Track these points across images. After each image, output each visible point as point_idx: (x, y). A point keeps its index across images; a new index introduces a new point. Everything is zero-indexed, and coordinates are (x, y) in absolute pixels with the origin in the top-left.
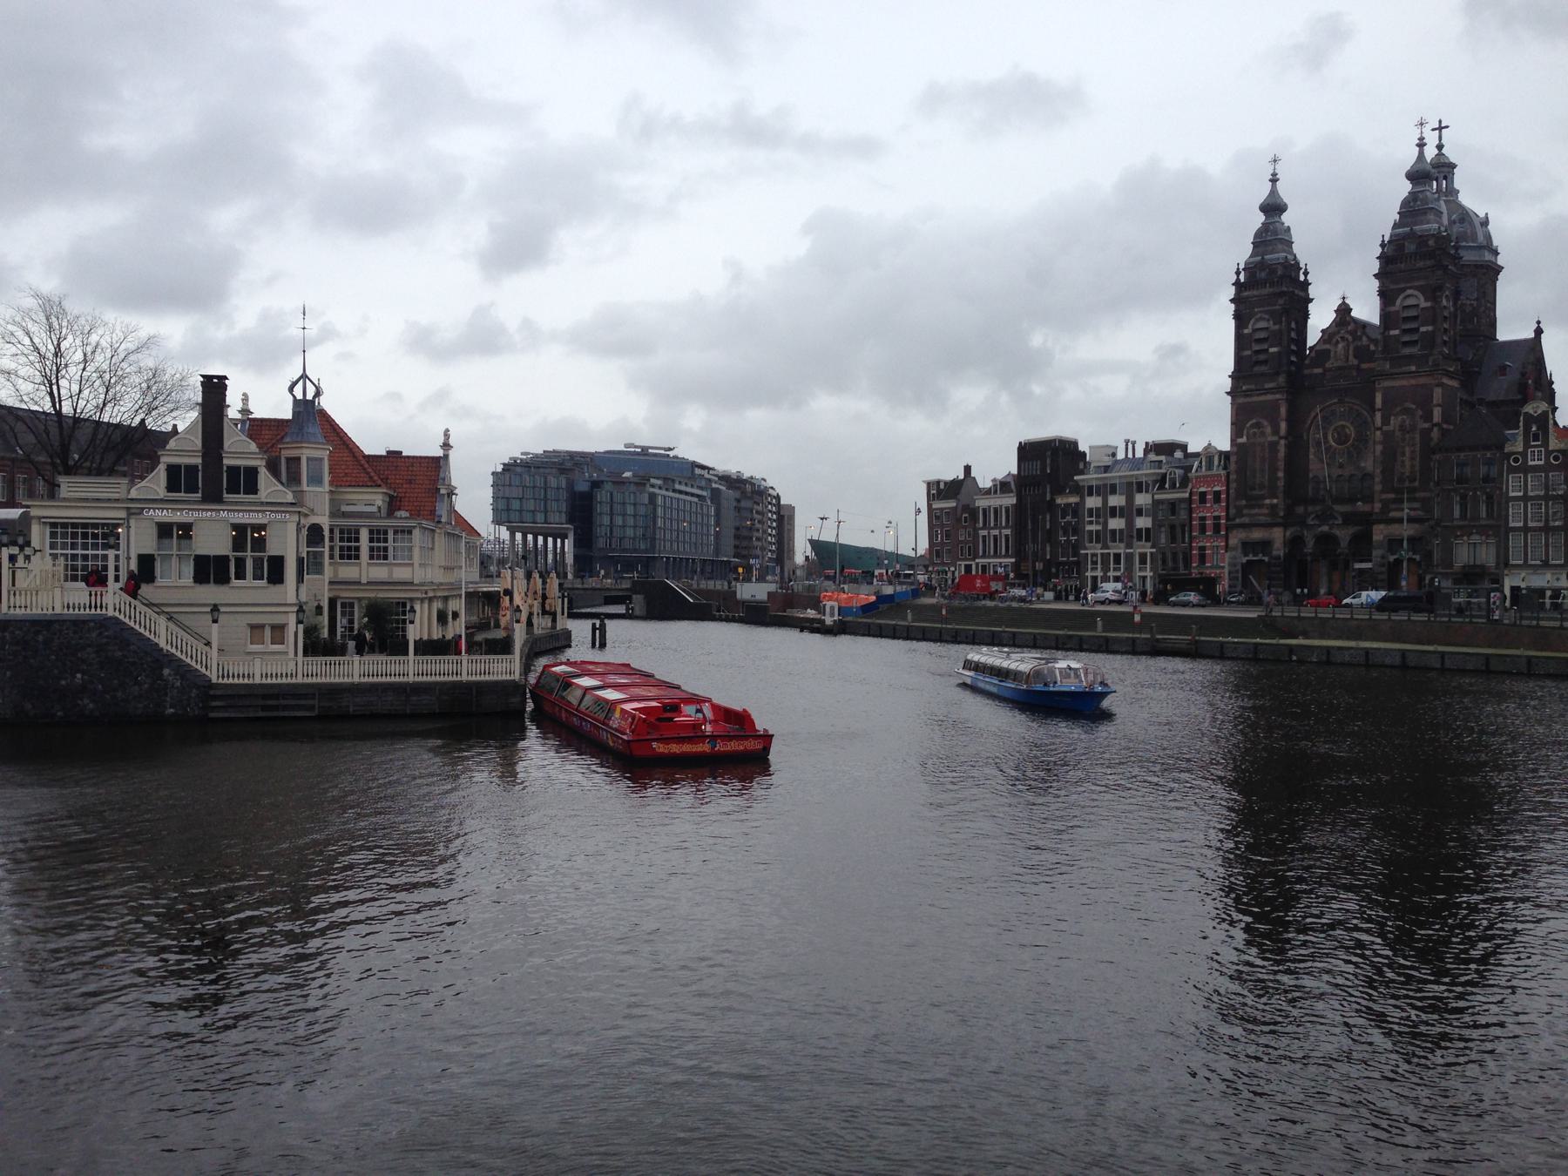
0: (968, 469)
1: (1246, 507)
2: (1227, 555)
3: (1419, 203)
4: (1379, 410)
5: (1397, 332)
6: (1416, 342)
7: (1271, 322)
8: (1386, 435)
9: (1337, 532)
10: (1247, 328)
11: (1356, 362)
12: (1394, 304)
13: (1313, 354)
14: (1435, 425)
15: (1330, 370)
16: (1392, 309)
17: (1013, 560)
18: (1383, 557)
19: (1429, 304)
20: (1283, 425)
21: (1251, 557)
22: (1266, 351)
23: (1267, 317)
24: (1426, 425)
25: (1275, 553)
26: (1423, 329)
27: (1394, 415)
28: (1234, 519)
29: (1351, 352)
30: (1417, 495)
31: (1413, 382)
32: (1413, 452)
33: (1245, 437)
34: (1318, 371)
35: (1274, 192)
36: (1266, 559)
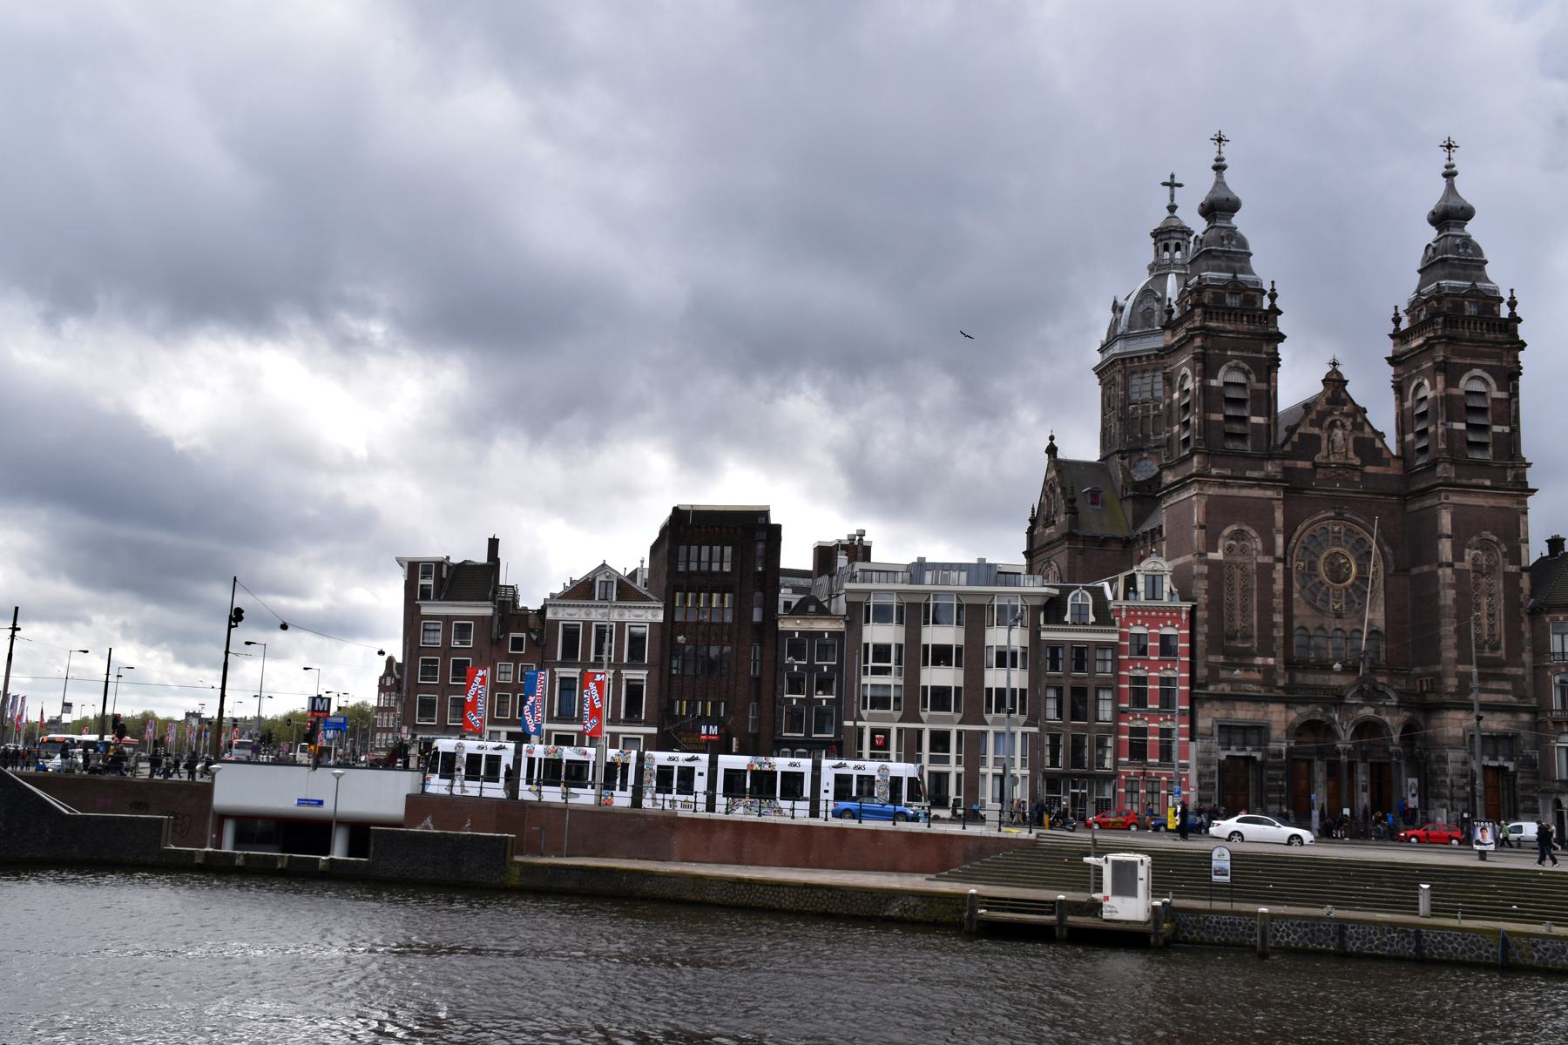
0: (493, 544)
1: (1224, 666)
2: (1194, 748)
3: (1470, 251)
4: (1448, 537)
5: (1462, 426)
6: (1482, 446)
7: (1253, 377)
8: (1459, 574)
9: (1387, 719)
10: (1216, 378)
11: (1357, 461)
12: (1457, 387)
13: (1295, 438)
14: (1524, 569)
15: (1326, 466)
16: (1454, 391)
17: (654, 730)
18: (1465, 763)
19: (1503, 395)
20: (1280, 540)
21: (1233, 751)
22: (1243, 420)
23: (1247, 367)
24: (1513, 569)
25: (1273, 746)
26: (1497, 429)
27: (1470, 547)
28: (1205, 686)
29: (1351, 445)
30: (1506, 670)
31: (1492, 502)
32: (1490, 605)
33: (1220, 552)
34: (1307, 465)
35: (1220, 183)
36: (1258, 756)
